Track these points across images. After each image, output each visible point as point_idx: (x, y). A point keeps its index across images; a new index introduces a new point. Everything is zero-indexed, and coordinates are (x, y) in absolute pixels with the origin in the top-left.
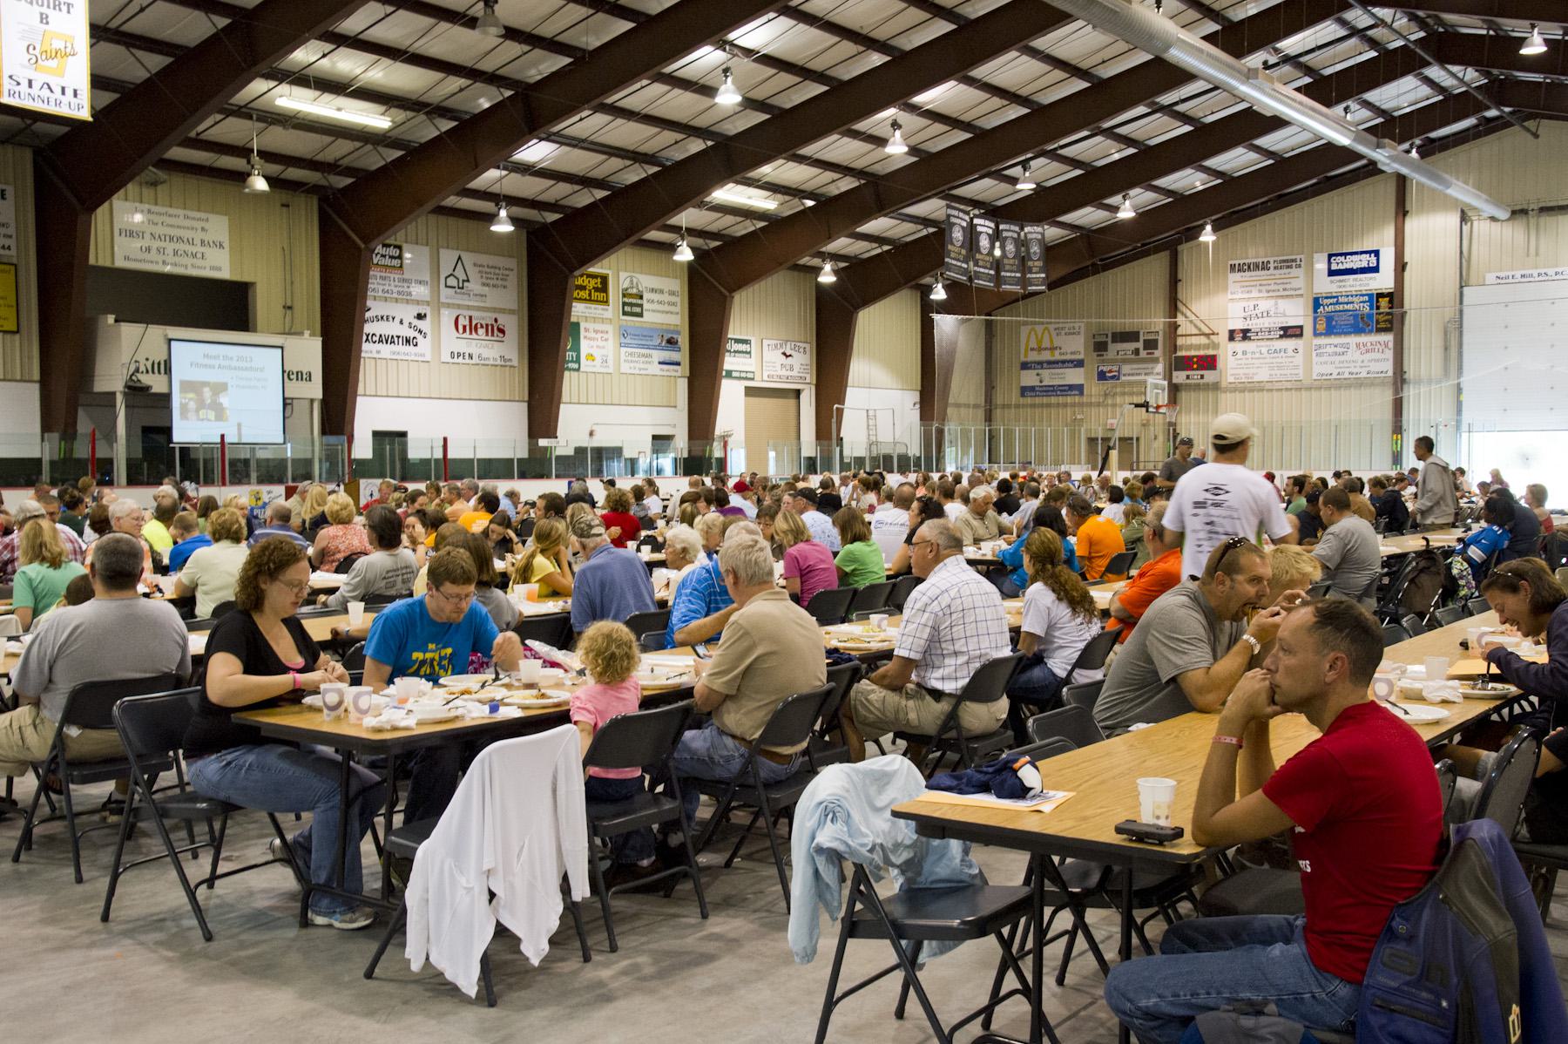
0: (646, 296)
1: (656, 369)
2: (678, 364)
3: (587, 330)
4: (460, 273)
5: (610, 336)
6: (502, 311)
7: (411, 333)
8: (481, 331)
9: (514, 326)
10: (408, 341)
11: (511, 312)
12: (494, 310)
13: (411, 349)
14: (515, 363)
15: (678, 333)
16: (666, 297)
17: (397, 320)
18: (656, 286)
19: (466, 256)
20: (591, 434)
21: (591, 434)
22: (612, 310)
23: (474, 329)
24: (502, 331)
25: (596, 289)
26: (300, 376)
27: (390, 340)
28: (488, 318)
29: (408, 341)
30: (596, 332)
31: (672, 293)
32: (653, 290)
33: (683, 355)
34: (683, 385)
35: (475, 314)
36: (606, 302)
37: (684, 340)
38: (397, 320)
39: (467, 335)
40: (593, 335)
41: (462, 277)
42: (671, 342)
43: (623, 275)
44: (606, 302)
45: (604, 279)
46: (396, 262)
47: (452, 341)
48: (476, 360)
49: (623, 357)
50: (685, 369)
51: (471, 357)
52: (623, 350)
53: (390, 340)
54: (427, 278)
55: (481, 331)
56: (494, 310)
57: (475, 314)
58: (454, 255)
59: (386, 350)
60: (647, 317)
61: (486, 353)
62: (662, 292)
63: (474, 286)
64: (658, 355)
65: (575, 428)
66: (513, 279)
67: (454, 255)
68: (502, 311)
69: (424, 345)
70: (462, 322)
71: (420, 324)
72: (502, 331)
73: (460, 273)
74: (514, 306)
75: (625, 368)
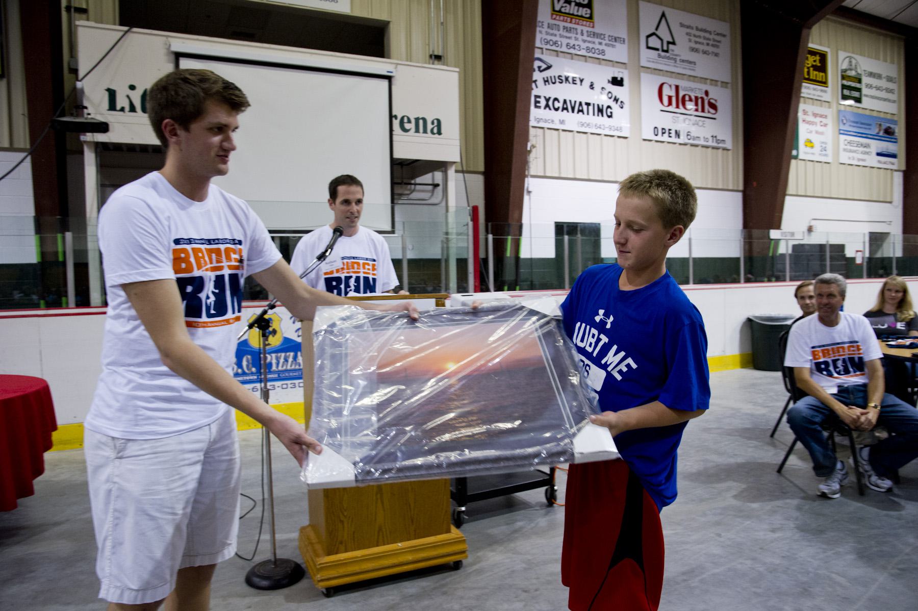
0: (865, 80)
1: (874, 160)
2: (894, 156)
3: (805, 112)
4: (663, 32)
5: (829, 121)
6: (714, 82)
7: (604, 100)
8: (690, 106)
9: (727, 100)
10: (600, 111)
11: (724, 84)
12: (704, 80)
13: (603, 120)
14: (729, 145)
15: (895, 122)
16: (883, 83)
17: (586, 84)
18: (875, 71)
19: (669, 12)
20: (810, 229)
21: (810, 229)
22: (831, 92)
23: (682, 102)
24: (713, 106)
25: (816, 68)
26: (421, 124)
27: (579, 108)
28: (697, 89)
29: (600, 111)
30: (815, 115)
31: (890, 79)
32: (871, 75)
33: (899, 148)
34: (898, 179)
35: (682, 83)
36: (824, 83)
37: (900, 131)
38: (586, 84)
39: (672, 108)
40: (810, 118)
41: (667, 38)
42: (889, 132)
43: (842, 55)
44: (824, 83)
45: (823, 57)
46: (584, 12)
47: (654, 114)
48: (683, 139)
49: (842, 146)
50: (899, 163)
51: (678, 134)
52: (843, 137)
53: (579, 108)
54: (623, 34)
55: (690, 106)
56: (704, 80)
57: (682, 83)
58: (657, 10)
59: (572, 120)
60: (866, 103)
61: (695, 131)
62: (879, 76)
63: (681, 49)
64: (876, 145)
65: (803, 219)
66: (725, 47)
67: (657, 10)
68: (714, 82)
69: (621, 119)
70: (667, 91)
71: (616, 90)
72: (713, 106)
73: (663, 32)
74: (727, 78)
75: (844, 158)
